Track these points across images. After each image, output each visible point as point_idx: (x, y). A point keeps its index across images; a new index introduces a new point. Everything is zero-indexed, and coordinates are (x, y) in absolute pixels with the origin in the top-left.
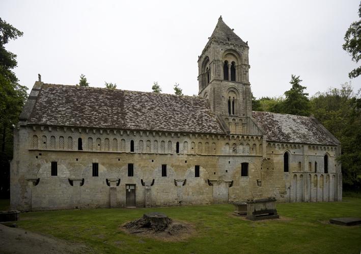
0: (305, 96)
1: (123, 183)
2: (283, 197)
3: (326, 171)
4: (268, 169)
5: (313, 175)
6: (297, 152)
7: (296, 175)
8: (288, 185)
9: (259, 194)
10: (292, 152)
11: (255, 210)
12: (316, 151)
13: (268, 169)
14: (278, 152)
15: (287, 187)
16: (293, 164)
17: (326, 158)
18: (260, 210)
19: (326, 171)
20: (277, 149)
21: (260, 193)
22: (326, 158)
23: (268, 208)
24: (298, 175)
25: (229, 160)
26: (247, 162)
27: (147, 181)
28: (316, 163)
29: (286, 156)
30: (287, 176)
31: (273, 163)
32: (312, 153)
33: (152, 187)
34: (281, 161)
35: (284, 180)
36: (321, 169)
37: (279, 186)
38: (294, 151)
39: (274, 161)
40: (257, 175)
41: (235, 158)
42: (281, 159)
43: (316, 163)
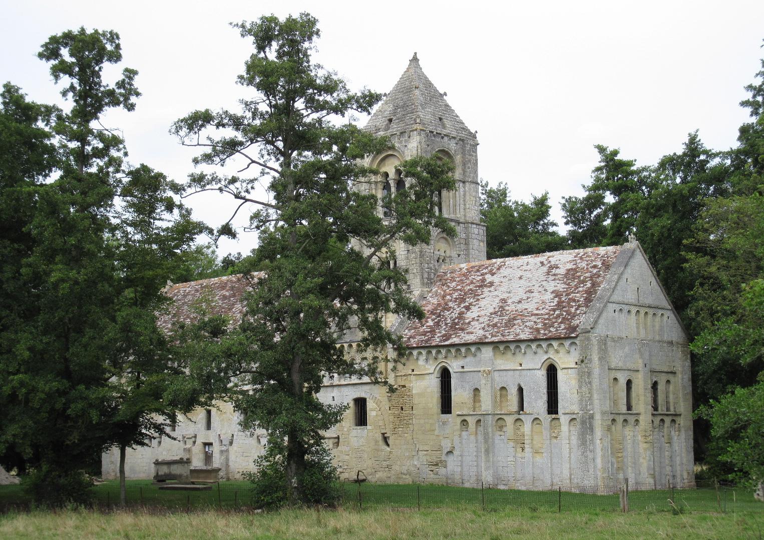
0: (453, 224)
1: (200, 441)
2: (437, 474)
3: (553, 406)
4: (402, 409)
5: (509, 420)
6: (470, 364)
7: (465, 420)
8: (446, 445)
9: (385, 464)
10: (454, 366)
11: (157, 473)
12: (519, 358)
13: (402, 409)
14: (425, 369)
15: (445, 451)
16: (459, 395)
17: (552, 372)
18: (163, 474)
19: (553, 406)
20: (421, 362)
21: (388, 463)
22: (552, 372)
23: (173, 472)
24: (471, 421)
25: (333, 395)
26: (363, 395)
27: (226, 439)
28: (521, 390)
29: (445, 376)
30: (444, 423)
31: (411, 396)
32: (506, 362)
33: (230, 448)
34: (428, 390)
35: (436, 433)
36: (537, 402)
37: (426, 448)
38: (461, 362)
39: (414, 392)
40: (381, 423)
41: (343, 389)
42: (433, 384)
43: (521, 390)
